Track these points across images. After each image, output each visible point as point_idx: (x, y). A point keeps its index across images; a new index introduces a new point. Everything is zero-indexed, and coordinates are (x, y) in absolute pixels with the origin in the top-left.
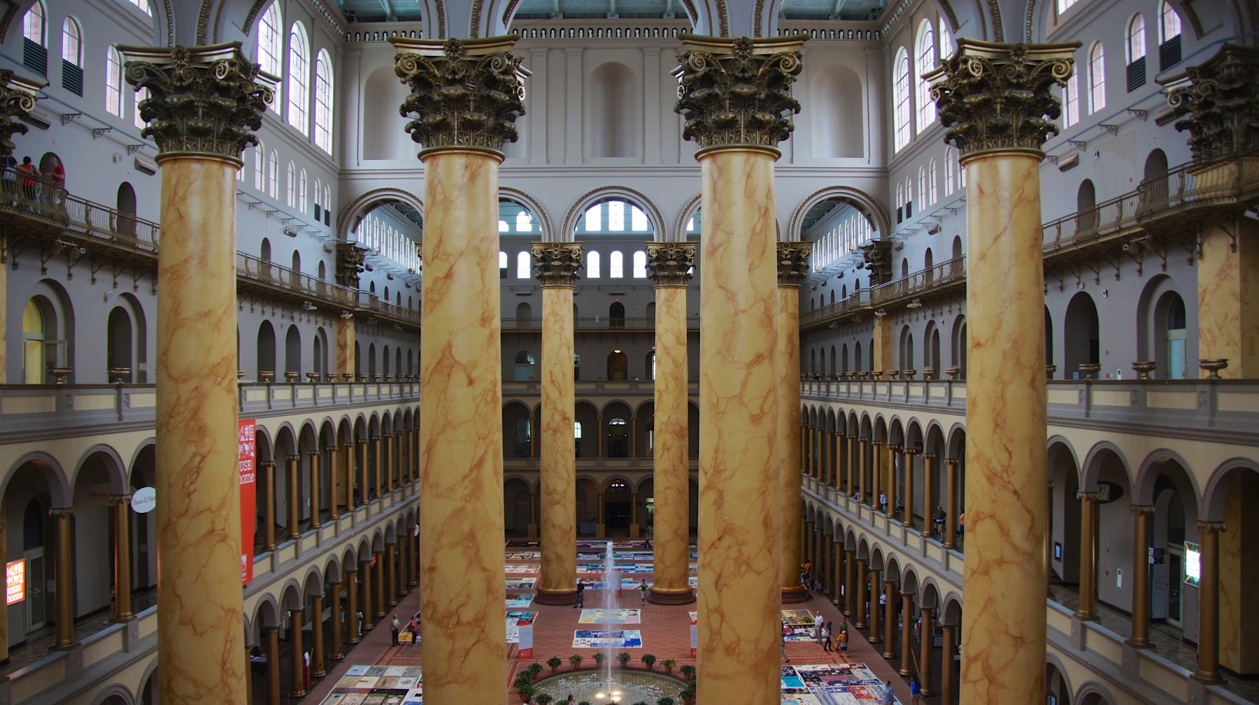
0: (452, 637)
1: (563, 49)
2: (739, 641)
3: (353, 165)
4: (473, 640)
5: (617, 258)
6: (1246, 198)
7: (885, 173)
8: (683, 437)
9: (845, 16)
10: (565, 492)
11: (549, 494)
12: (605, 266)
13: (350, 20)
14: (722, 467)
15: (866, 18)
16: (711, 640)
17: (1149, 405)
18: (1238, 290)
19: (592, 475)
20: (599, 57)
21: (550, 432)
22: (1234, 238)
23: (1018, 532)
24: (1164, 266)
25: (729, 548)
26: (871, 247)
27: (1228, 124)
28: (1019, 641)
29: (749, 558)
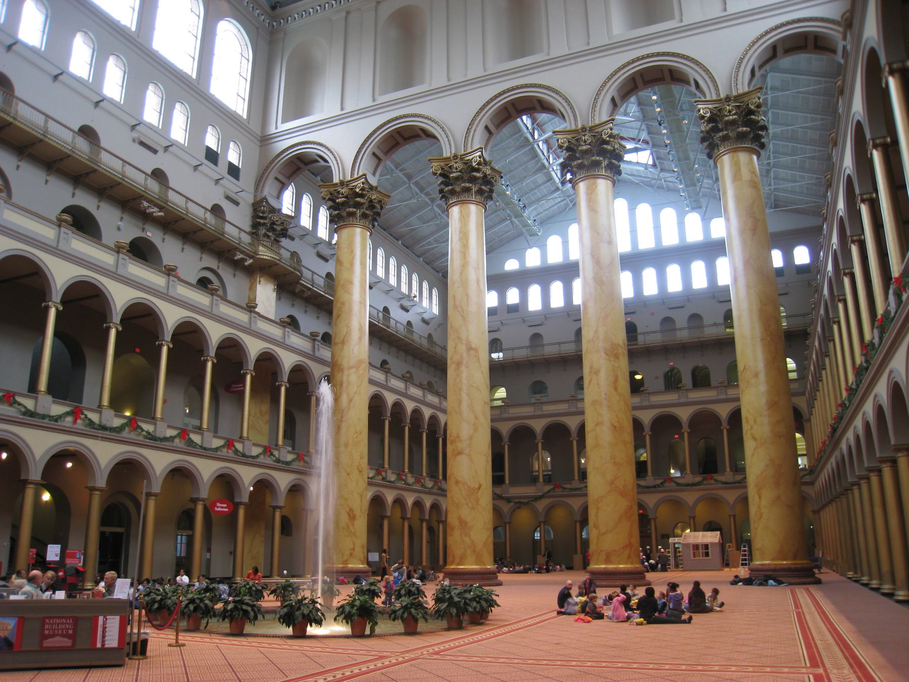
3: (272, 130)
8: (617, 357)
10: (471, 438)
13: (273, 8)
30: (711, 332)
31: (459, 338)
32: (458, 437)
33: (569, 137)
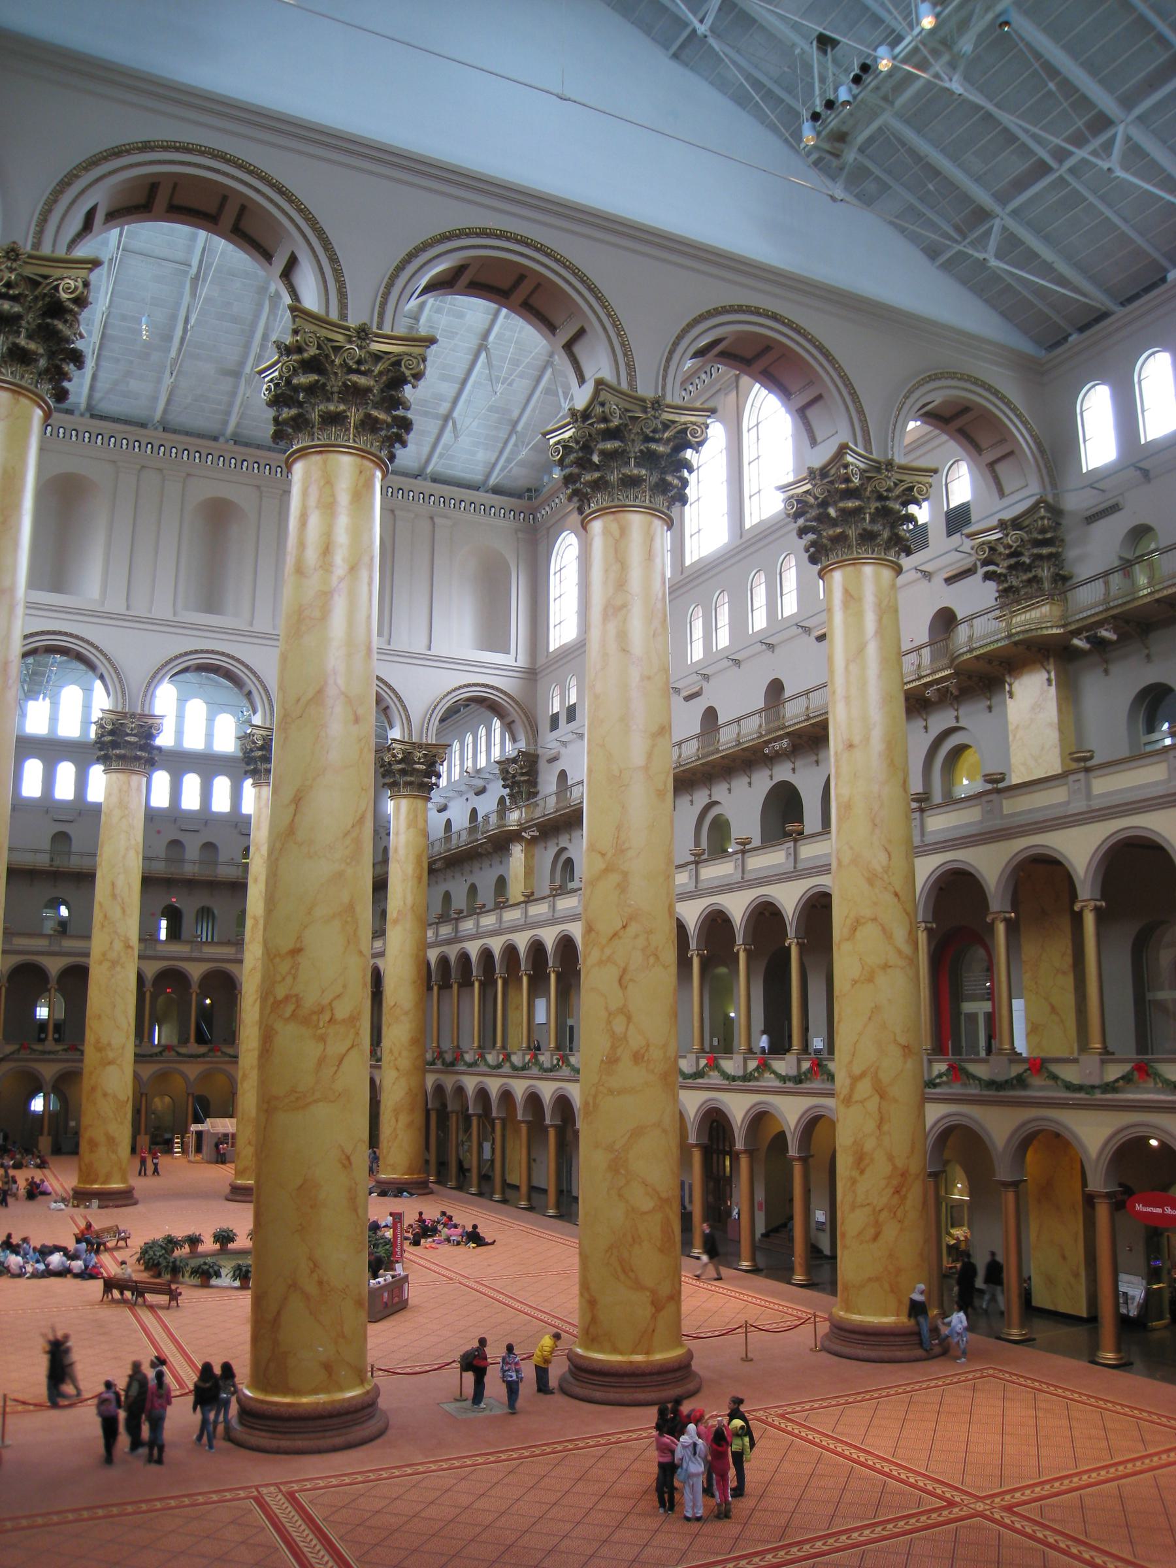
0: (322, 1039)
1: (160, 470)
2: (648, 1045)
4: (348, 1043)
6: (1073, 627)
7: (531, 675)
9: (497, 491)
11: (99, 1049)
14: (626, 845)
15: (520, 496)
16: (614, 1047)
17: (1005, 812)
18: (1055, 720)
20: (206, 488)
21: (107, 964)
22: (1049, 672)
23: (900, 934)
24: (957, 718)
25: (636, 936)
26: (514, 760)
27: (1039, 572)
28: (907, 1049)
29: (657, 948)
30: (226, 872)
31: (116, 932)
32: (109, 1044)
33: (264, 733)
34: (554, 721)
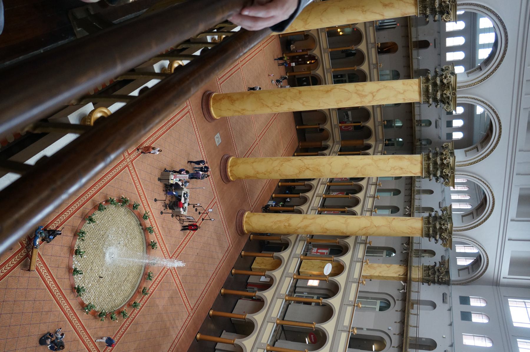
5: (460, 41)
7: (496, 283)
12: (454, 34)
19: (318, 46)
34: (465, 300)
